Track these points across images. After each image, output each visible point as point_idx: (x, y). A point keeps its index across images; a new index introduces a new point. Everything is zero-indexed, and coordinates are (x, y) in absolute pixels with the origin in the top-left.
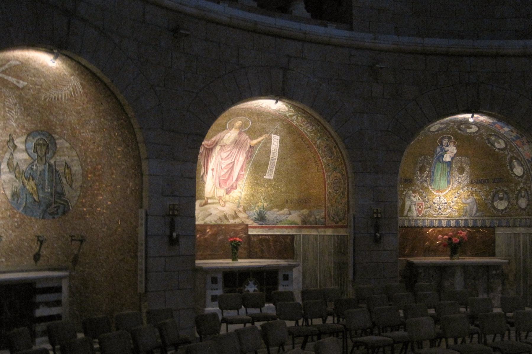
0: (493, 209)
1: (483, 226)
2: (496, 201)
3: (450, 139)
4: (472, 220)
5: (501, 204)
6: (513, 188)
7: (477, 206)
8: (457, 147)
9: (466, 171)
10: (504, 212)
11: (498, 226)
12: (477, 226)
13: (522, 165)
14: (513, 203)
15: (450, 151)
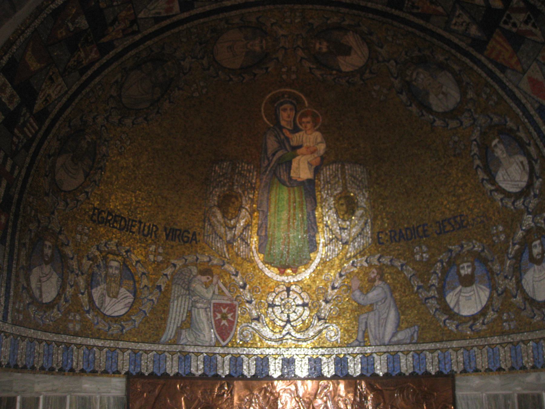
0: (446, 317)
1: (417, 370)
2: (454, 289)
3: (297, 104)
4: (384, 357)
5: (468, 298)
6: (502, 237)
7: (397, 309)
8: (324, 130)
9: (362, 207)
10: (478, 325)
11: (464, 371)
12: (401, 375)
13: (523, 148)
14: (505, 290)
15: (308, 148)
